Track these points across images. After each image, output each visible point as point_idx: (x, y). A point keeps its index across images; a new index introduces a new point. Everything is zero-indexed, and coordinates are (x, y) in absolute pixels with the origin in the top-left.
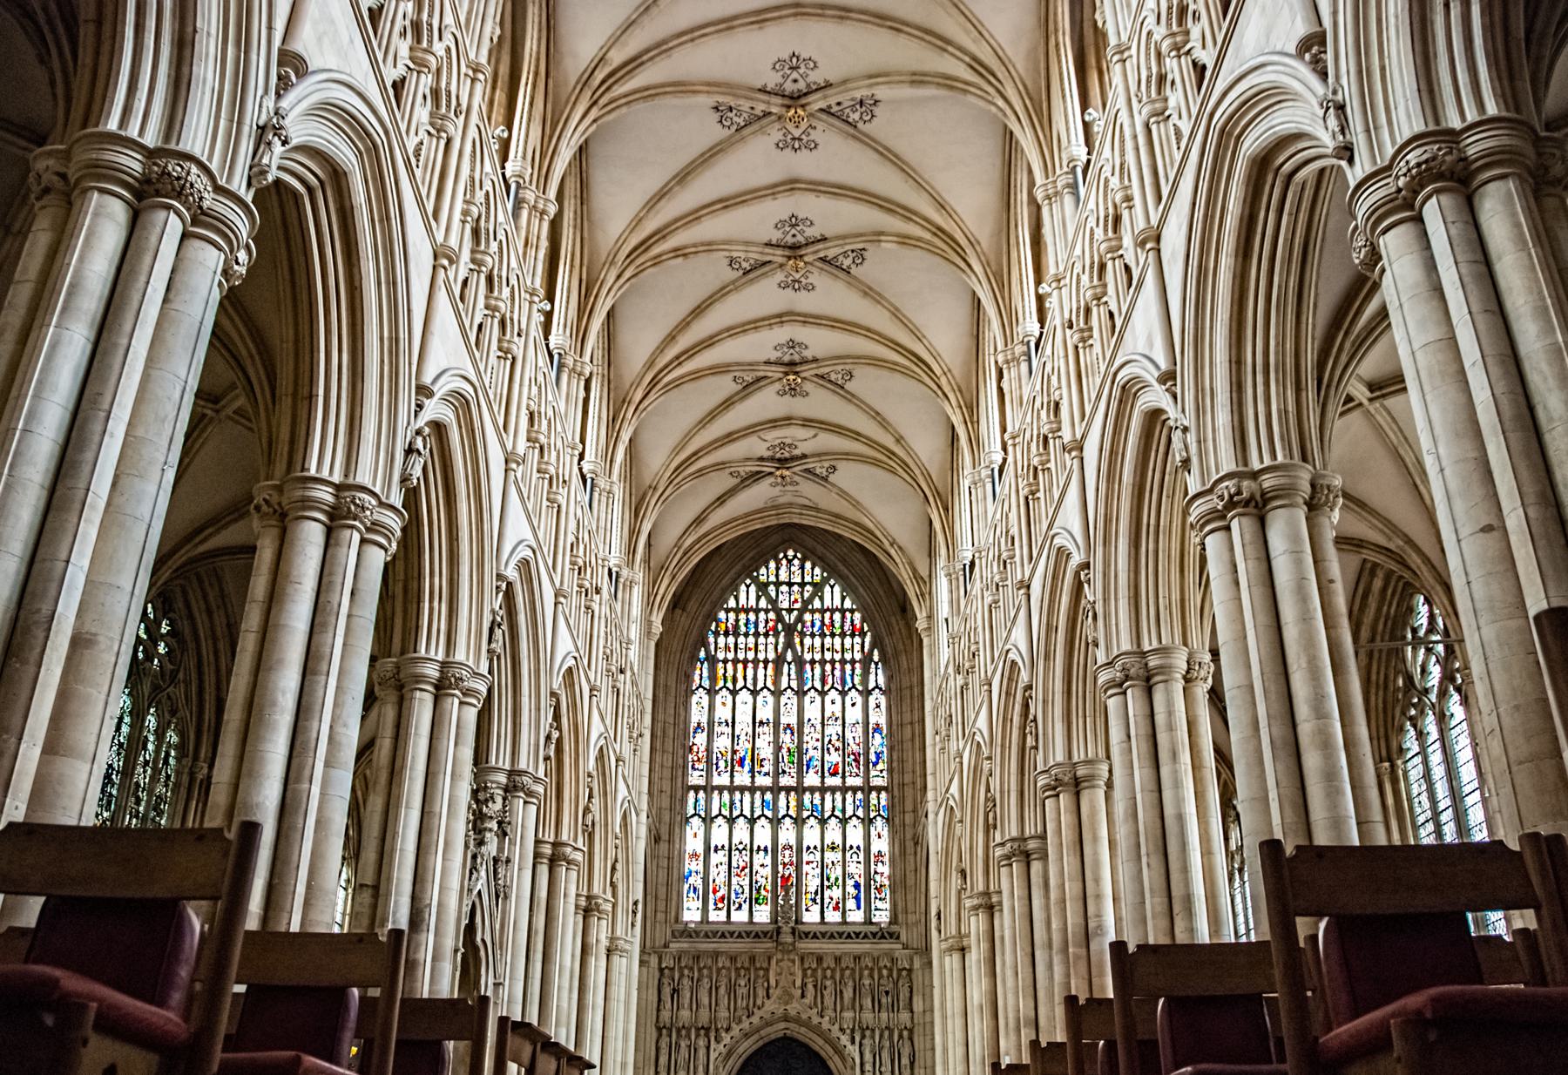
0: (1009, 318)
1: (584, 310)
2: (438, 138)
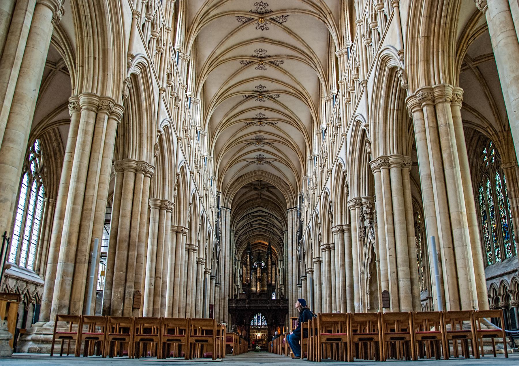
0: (328, 88)
1: (197, 84)
2: (159, 54)
